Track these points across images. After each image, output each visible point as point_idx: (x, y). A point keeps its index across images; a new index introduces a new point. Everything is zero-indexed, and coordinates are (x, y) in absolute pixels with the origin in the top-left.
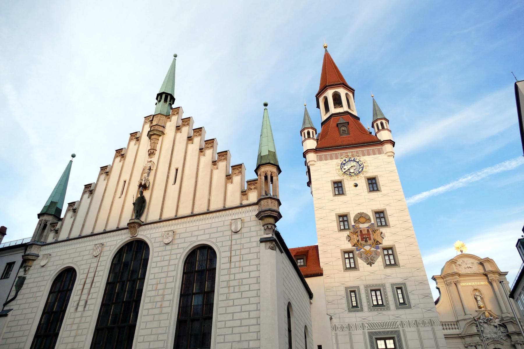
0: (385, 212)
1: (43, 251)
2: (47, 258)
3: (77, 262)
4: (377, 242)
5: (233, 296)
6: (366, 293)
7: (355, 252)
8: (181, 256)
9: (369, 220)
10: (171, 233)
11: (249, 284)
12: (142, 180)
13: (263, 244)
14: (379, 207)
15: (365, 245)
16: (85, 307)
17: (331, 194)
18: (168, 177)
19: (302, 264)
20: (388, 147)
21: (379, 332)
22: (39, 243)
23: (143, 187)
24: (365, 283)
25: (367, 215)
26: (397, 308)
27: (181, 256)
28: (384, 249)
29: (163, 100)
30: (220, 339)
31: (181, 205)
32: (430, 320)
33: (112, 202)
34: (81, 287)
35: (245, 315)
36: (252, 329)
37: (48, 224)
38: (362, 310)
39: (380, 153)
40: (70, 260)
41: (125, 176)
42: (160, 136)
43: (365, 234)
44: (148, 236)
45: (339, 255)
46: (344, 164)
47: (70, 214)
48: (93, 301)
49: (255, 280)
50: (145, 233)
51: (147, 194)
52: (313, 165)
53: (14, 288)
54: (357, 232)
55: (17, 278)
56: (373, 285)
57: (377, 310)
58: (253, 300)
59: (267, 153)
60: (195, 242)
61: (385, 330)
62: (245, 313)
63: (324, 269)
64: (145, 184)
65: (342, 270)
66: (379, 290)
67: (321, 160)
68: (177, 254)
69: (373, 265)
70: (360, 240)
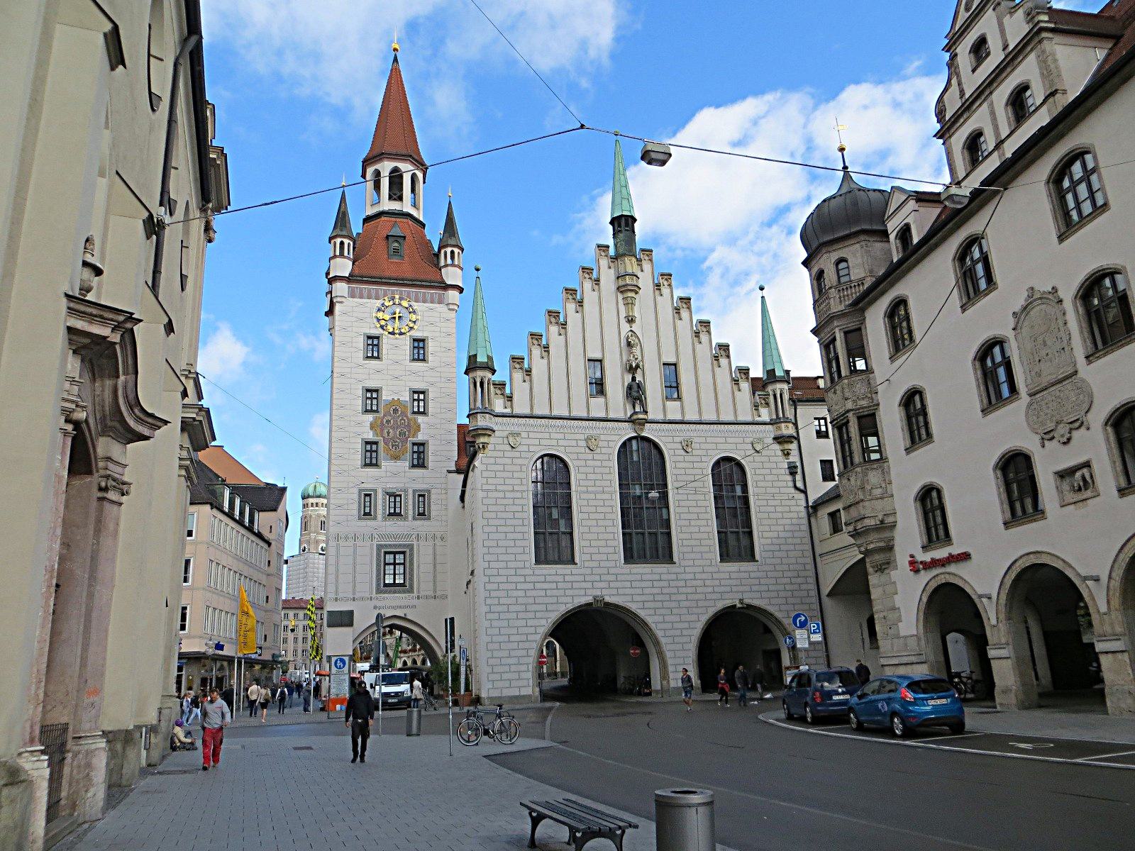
7: (379, 444)
17: (361, 354)
20: (453, 295)
38: (375, 518)
39: (440, 302)
45: (359, 446)
52: (341, 302)
66: (400, 496)
67: (352, 295)
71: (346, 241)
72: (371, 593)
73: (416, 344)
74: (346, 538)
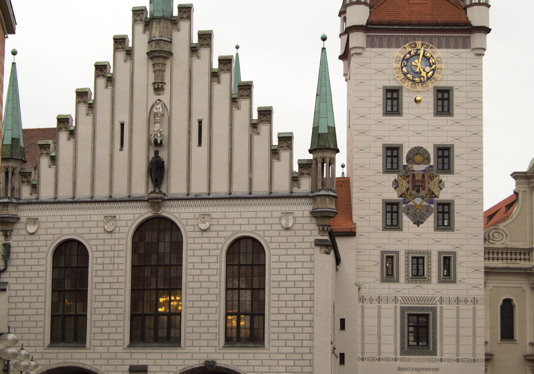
0: (451, 149)
3: (83, 234)
4: (433, 193)
6: (406, 261)
7: (400, 205)
8: (223, 247)
9: (428, 159)
11: (303, 288)
13: (318, 249)
14: (443, 141)
15: (415, 197)
17: (380, 110)
21: (413, 308)
24: (407, 248)
25: (426, 152)
26: (440, 281)
28: (439, 204)
31: (214, 180)
32: (474, 298)
35: (299, 317)
37: (17, 171)
38: (397, 281)
40: (72, 231)
42: (166, 58)
43: (419, 181)
44: (177, 215)
45: (380, 207)
46: (407, 60)
50: (172, 211)
51: (163, 155)
54: (408, 176)
56: (416, 251)
57: (416, 282)
60: (238, 232)
61: (421, 305)
63: (357, 225)
65: (381, 228)
67: (372, 47)
68: (217, 243)
69: (421, 225)
70: (410, 188)
72: (396, 354)
73: (440, 96)
74: (371, 300)
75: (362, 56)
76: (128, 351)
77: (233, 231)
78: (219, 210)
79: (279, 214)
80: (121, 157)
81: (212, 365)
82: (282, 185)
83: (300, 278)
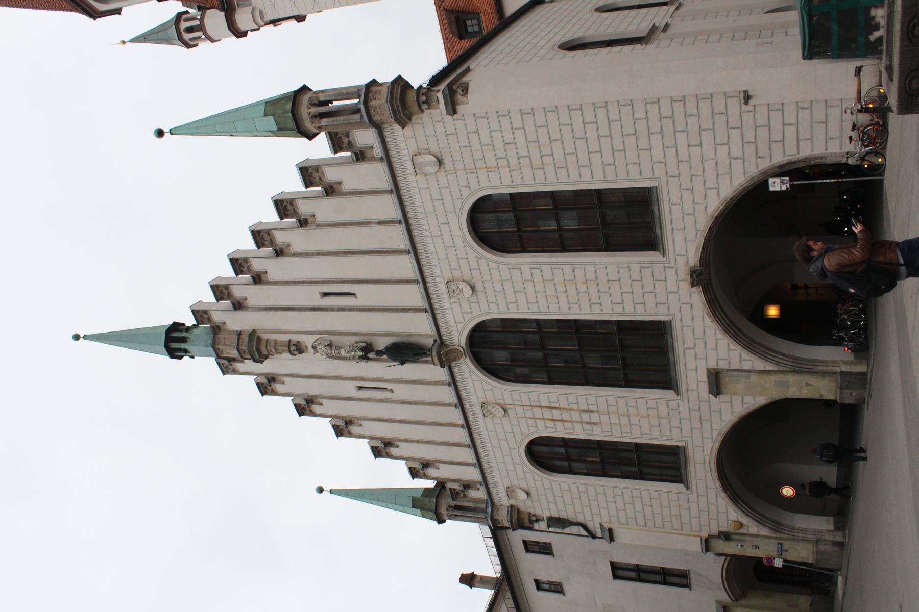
1: (502, 499)
2: (513, 491)
3: (516, 441)
5: (559, 156)
8: (493, 261)
10: (453, 286)
12: (354, 358)
13: (460, 108)
16: (592, 411)
18: (342, 309)
19: (475, 22)
22: (489, 510)
23: (367, 351)
27: (493, 261)
29: (183, 346)
30: (634, 172)
33: (403, 403)
34: (559, 424)
35: (591, 129)
36: (614, 115)
37: (453, 503)
40: (515, 453)
41: (349, 389)
42: (259, 339)
44: (460, 326)
47: (431, 471)
48: (582, 400)
49: (528, 119)
51: (382, 343)
53: (567, 530)
55: (551, 529)
58: (564, 119)
59: (271, 118)
60: (464, 240)
62: (588, 132)
64: (362, 349)
71: (183, 25)
75: (263, 9)
76: (685, 395)
77: (465, 247)
78: (438, 268)
79: (422, 180)
80: (401, 392)
81: (698, 276)
82: (374, 174)
83: (519, 134)
